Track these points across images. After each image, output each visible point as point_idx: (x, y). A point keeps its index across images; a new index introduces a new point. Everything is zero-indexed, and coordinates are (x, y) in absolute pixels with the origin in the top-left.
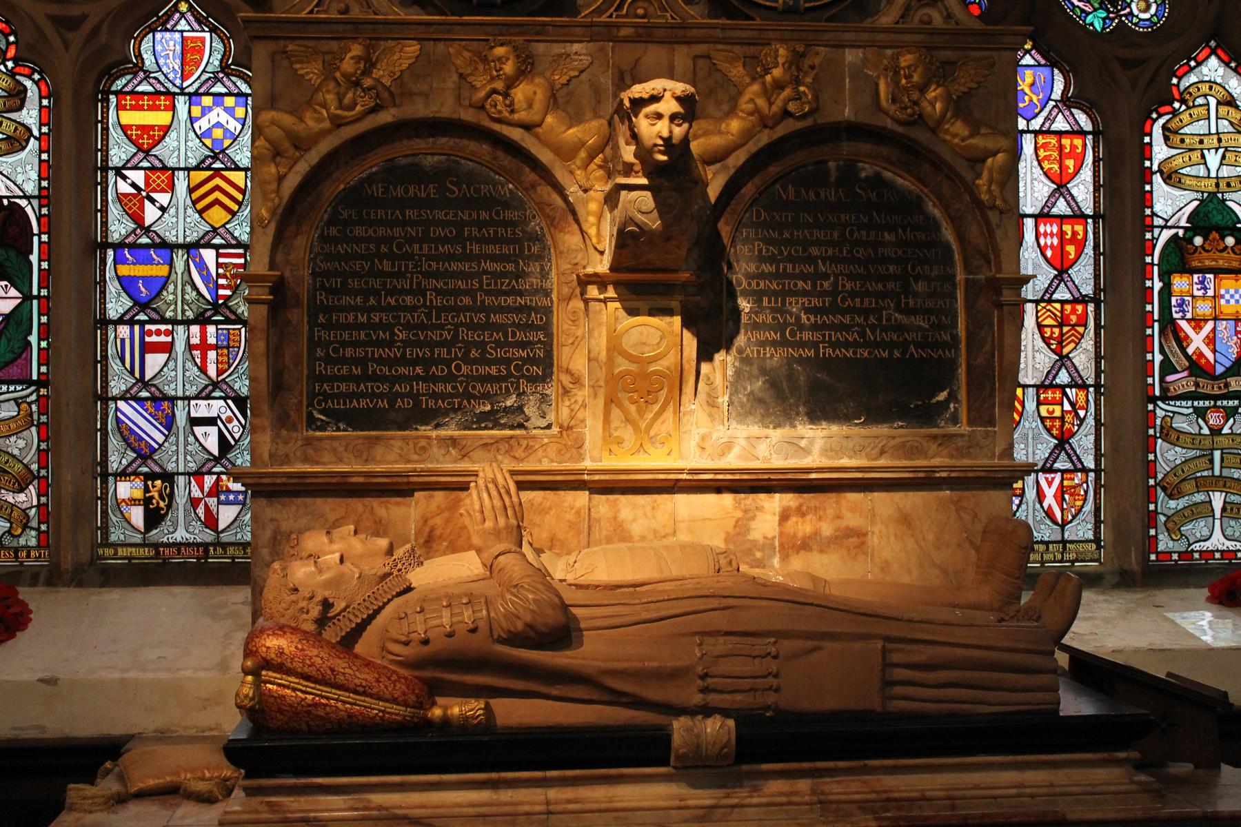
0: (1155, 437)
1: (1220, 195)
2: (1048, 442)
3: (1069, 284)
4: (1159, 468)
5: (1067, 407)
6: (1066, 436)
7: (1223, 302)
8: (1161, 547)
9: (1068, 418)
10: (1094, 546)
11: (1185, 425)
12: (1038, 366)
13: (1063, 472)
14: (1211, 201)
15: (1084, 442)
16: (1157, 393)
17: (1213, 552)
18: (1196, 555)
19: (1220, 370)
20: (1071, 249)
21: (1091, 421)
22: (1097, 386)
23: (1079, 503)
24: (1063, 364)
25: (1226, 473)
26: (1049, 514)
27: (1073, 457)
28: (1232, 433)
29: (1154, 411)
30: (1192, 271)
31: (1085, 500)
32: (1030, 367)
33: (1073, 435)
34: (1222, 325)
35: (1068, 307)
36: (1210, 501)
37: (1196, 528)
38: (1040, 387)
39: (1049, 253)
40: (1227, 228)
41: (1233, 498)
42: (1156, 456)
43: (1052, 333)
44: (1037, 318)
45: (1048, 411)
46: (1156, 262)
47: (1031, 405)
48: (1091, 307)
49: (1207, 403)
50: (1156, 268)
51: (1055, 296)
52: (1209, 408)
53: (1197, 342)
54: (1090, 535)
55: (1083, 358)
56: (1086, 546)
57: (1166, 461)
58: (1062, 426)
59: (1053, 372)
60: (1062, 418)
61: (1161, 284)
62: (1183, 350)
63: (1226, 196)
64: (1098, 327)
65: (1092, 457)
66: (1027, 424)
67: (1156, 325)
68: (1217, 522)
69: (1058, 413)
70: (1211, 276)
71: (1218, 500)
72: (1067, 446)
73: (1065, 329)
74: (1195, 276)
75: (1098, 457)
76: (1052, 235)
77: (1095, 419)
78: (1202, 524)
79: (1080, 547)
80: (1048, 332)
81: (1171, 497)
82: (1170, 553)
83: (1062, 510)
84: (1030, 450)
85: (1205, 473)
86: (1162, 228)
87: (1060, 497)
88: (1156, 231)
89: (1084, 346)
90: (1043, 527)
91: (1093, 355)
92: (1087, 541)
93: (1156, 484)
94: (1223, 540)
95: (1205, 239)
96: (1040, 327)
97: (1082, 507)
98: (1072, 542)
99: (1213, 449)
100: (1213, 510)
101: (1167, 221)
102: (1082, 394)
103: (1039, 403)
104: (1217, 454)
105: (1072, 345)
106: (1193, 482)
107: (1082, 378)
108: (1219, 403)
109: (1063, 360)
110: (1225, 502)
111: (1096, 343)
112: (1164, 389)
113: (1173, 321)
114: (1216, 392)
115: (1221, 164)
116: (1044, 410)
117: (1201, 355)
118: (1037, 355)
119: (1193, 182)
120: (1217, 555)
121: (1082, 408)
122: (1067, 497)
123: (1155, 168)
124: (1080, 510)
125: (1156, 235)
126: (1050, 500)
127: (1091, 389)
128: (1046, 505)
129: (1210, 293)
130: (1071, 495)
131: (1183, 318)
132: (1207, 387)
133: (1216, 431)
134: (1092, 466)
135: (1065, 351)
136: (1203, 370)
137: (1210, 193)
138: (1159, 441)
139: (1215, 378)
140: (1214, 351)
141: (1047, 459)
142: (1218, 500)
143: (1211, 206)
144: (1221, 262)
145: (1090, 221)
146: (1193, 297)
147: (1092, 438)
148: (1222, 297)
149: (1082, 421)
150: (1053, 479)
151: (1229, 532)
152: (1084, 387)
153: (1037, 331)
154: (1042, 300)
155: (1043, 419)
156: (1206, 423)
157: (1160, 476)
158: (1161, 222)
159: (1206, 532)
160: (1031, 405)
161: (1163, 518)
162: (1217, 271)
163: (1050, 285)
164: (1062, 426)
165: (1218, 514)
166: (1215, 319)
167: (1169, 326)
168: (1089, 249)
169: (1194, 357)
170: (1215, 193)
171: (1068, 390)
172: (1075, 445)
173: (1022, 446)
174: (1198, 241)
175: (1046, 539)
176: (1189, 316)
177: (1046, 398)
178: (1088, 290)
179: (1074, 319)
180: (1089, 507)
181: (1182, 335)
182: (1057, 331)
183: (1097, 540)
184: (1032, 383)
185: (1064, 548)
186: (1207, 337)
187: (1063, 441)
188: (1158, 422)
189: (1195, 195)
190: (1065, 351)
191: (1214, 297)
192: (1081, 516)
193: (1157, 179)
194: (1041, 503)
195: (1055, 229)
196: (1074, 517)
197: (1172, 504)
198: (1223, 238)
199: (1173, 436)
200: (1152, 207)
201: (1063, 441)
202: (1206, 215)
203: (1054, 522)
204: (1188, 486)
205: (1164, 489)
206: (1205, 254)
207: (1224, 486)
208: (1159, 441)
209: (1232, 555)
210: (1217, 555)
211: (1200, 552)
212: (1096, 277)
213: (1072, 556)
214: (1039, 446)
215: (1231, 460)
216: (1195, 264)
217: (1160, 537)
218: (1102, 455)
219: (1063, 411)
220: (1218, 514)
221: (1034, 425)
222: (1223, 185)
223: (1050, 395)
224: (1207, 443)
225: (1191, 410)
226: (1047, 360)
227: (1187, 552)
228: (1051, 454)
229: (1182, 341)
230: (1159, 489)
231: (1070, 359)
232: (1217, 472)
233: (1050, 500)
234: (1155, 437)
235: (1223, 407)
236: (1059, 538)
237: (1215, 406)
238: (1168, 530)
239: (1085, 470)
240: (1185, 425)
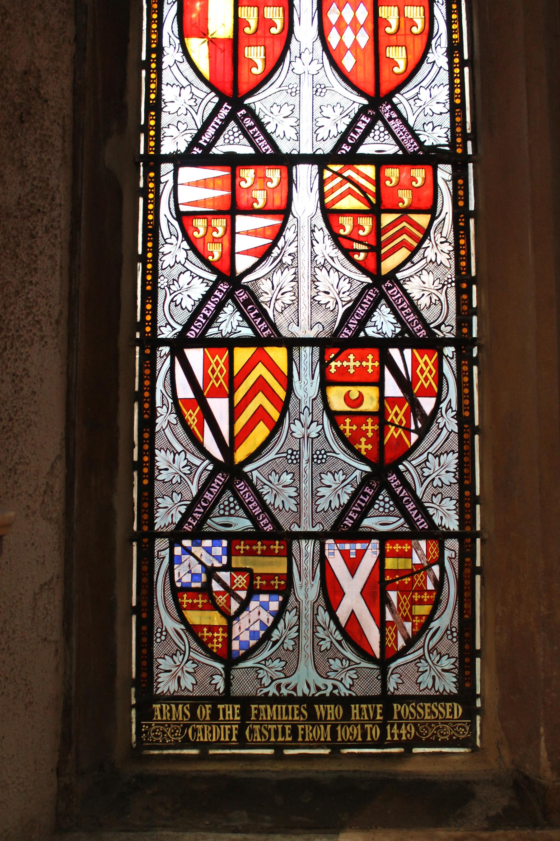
2: (347, 470)
3: (395, 125)
5: (392, 389)
6: (389, 456)
9: (396, 415)
10: (459, 710)
12: (323, 298)
13: (384, 538)
15: (434, 469)
20: (398, 56)
21: (448, 422)
22: (462, 343)
23: (425, 610)
24: (382, 296)
26: (351, 633)
27: (409, 504)
31: (436, 604)
32: (305, 301)
33: (408, 452)
35: (392, 174)
38: (329, 345)
39: (348, 62)
43: (357, 227)
44: (322, 196)
45: (347, 398)
47: (306, 387)
48: (444, 173)
51: (363, 150)
54: (449, 684)
55: (429, 283)
56: (439, 708)
58: (381, 433)
59: (359, 310)
60: (380, 415)
64: (460, 213)
65: (450, 504)
66: (298, 430)
69: (370, 403)
72: (392, 478)
73: (387, 219)
75: (466, 506)
76: (355, 25)
77: (459, 416)
79: (426, 711)
80: (347, 223)
83: (382, 625)
84: (306, 486)
87: (375, 593)
89: (430, 254)
90: (336, 664)
91: (451, 274)
92: (443, 698)
96: (329, 214)
97: (430, 618)
98: (405, 699)
102: (427, 362)
103: (326, 382)
105: (403, 253)
107: (426, 325)
109: (381, 286)
111: (457, 248)
116: (337, 398)
118: (321, 274)
121: (427, 393)
122: (393, 595)
124: (424, 627)
126: (353, 602)
127: (449, 351)
128: (343, 614)
130: (403, 590)
134: (453, 524)
135: (388, 265)
141: (346, 508)
147: (452, 460)
149: (429, 421)
150: (361, 554)
152: (431, 343)
153: (320, 222)
154: (333, 157)
155: (335, 417)
160: (306, 387)
163: (352, 127)
164: (381, 433)
168: (438, 55)
171: (394, 353)
172: (413, 477)
173: (287, 478)
175: (344, 692)
177: (343, 370)
178: (437, 135)
179: (406, 197)
180: (446, 619)
182: (367, 223)
183: (465, 695)
184: (311, 334)
185: (388, 713)
187: (384, 468)
190: (388, 265)
192: (427, 641)
194: (332, 610)
195: (363, 13)
196: (410, 642)
201: (384, 468)
203: (364, 652)
212: (456, 109)
213: (406, 732)
214: (328, 479)
218: (475, 500)
219: (382, 398)
221: (314, 430)
223: (351, 362)
226: (345, 285)
228: (354, 496)
231: (399, 284)
233: (353, 602)
236: (377, 691)
239: (437, 535)
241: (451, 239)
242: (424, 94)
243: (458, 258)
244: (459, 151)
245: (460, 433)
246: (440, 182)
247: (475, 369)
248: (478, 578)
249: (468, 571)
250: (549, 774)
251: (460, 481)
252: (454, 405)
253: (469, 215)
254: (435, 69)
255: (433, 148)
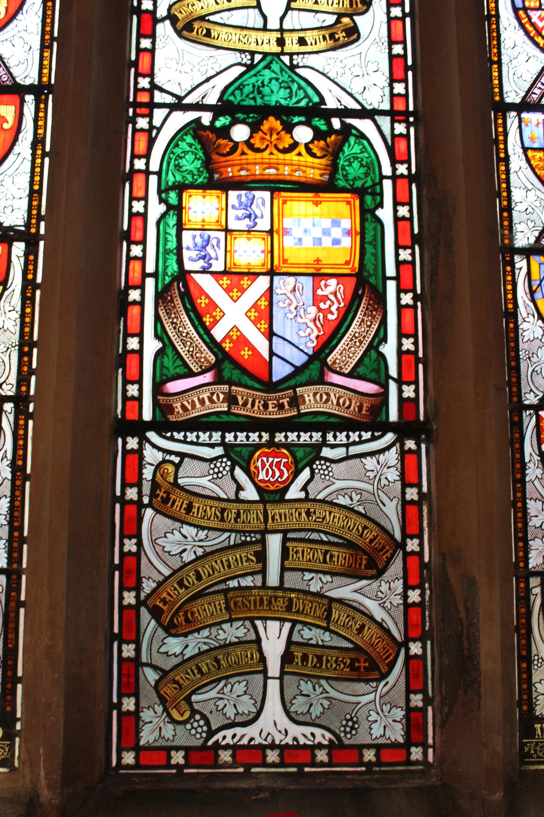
0: (139, 505)
1: (286, 59)
4: (145, 569)
7: (288, 242)
8: (147, 736)
11: (204, 481)
14: (268, 67)
16: (147, 415)
17: (262, 748)
18: (225, 756)
19: (280, 371)
25: (293, 580)
28: (307, 499)
29: (139, 452)
30: (225, 186)
34: (284, 285)
36: (258, 641)
37: (224, 699)
40: (298, 111)
41: (307, 633)
42: (140, 544)
46: (154, 166)
49: (254, 437)
50: (153, 180)
52: (257, 447)
53: (233, 317)
57: (163, 554)
61: (163, 208)
62: (205, 331)
63: (297, 60)
64: (28, 284)
67: (150, 283)
68: (273, 686)
70: (267, 195)
71: (274, 640)
74: (233, 194)
78: (240, 688)
81: (171, 630)
82: (168, 750)
85: (247, 582)
86: (173, 108)
88: (159, 114)
91: (15, 339)
93: (140, 603)
94: (284, 722)
95: (255, 128)
99: (265, 532)
100: (263, 659)
101: (180, 98)
104: (274, 543)
106: (220, 600)
108: (280, 437)
110: (289, 642)
111: (23, 316)
112: (162, 407)
113: (183, 275)
114: (272, 413)
115: (288, 8)
117: (242, 341)
119: (233, 38)
120: (272, 756)
123: (162, 12)
125: (157, 122)
129: (264, 224)
131: (204, 271)
132: (252, 403)
133: (273, 495)
136: (244, 371)
137: (265, 55)
138: (149, 513)
139: (270, 387)
140: (270, 334)
142: (274, 640)
143: (267, 74)
144: (286, 170)
145: (30, 98)
146: (227, 230)
148: (286, 232)
151: (299, 705)
156: (252, 477)
157: (148, 586)
158: (169, 99)
159: (247, 706)
161: (152, 676)
162: (276, 186)
165: (274, 667)
166: (272, 273)
167: (179, 290)
169: (227, 346)
170: (278, 55)
174: (240, 133)
176: (218, 266)
181: (202, 302)
186: (255, 306)
188: (148, 473)
189: (235, 57)
191: (271, 232)
193: (164, 30)
197: (174, 645)
198: (289, 128)
199: (180, 502)
200: (151, 75)
202: (258, 90)
204: (205, 609)
205: (156, 613)
206: (251, 156)
207: (289, 609)
208: (149, 513)
209: (305, 757)
210: (272, 756)
211: (235, 748)
212: (34, 194)
215: (303, 553)
216: (230, 172)
217: (146, 715)
218: (22, 540)
220: (274, 667)
222: (291, 46)
224: (253, 519)
225: (219, 451)
227: (204, 747)
229: (201, 318)
230: (144, 613)
232: (273, 579)
234: (139, 505)
235: (287, 446)
237: (271, 443)
238: (163, 701)
240: (204, 481)
241: (19, 308)
242: (7, 181)
243: (23, 324)
244: (33, 231)
245: (13, 481)
246: (14, 258)
247: (31, 423)
248: (22, 611)
249: (13, 604)
250: (46, 792)
251: (10, 523)
252: (10, 455)
253: (36, 286)
254: (20, 159)
255: (11, 228)
